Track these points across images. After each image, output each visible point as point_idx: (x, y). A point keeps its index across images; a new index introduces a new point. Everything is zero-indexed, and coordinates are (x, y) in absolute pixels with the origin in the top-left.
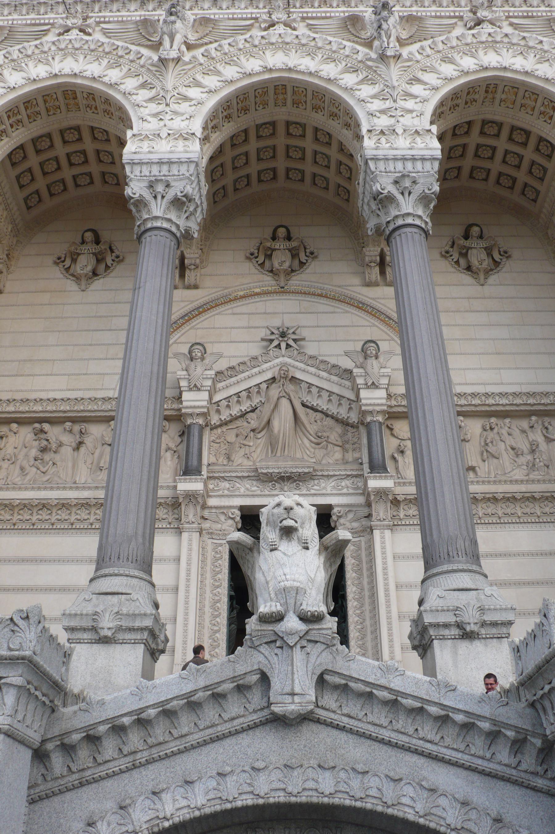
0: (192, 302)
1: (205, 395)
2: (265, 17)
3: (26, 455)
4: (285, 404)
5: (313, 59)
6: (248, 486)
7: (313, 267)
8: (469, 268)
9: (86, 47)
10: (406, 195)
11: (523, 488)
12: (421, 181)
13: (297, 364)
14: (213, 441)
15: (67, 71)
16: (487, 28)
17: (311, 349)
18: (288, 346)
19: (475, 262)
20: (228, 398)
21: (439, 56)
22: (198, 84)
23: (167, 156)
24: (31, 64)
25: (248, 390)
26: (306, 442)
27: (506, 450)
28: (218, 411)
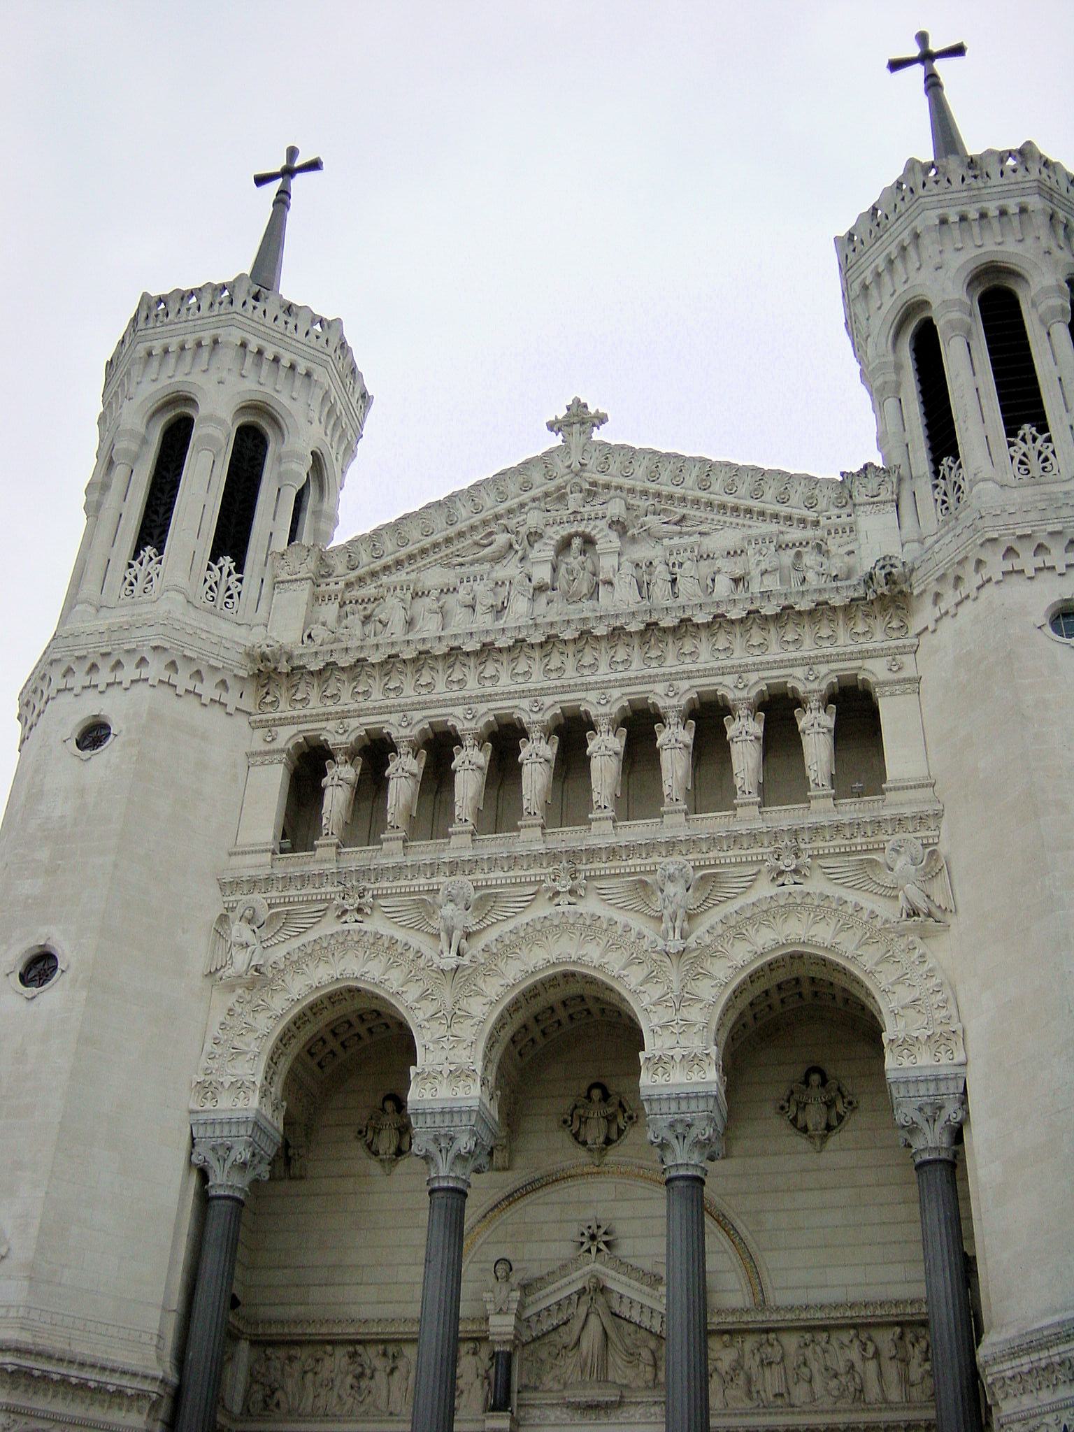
1: (510, 1320)
2: (549, 883)
3: (342, 1382)
5: (598, 944)
8: (805, 1130)
9: (365, 939)
10: (681, 1140)
12: (696, 1123)
14: (526, 1359)
15: (348, 973)
18: (599, 1250)
20: (538, 1314)
21: (732, 932)
22: (480, 993)
23: (448, 1104)
25: (558, 1304)
26: (619, 1362)
28: (529, 1327)
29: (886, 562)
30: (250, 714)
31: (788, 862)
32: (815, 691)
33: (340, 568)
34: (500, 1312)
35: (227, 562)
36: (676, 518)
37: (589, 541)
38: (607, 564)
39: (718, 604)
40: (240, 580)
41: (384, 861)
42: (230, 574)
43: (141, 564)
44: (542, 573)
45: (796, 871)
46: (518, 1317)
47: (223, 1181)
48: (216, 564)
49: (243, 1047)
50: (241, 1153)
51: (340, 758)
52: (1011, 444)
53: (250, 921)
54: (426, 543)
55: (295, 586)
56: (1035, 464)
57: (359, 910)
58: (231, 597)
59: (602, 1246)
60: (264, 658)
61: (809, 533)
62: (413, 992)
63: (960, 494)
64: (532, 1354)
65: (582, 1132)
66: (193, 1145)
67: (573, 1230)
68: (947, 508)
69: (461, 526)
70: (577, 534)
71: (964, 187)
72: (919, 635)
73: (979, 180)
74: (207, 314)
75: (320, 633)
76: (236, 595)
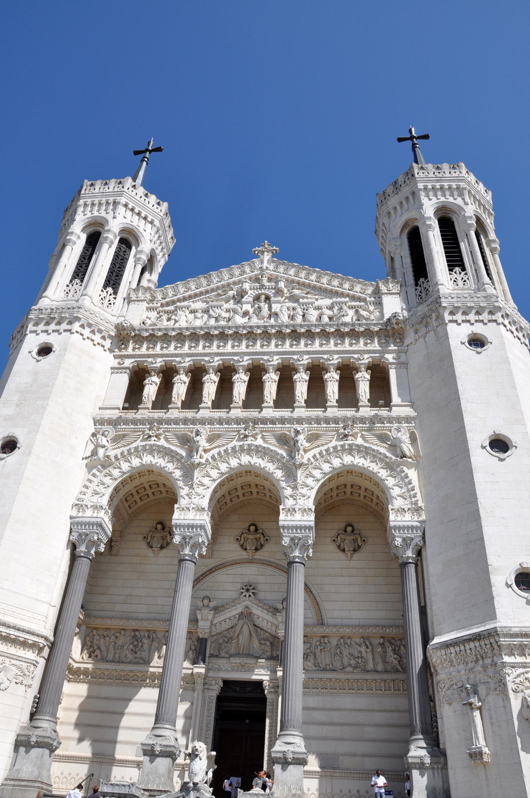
0: (207, 566)
1: (208, 624)
3: (128, 649)
4: (245, 627)
6: (226, 667)
7: (266, 548)
8: (344, 551)
11: (349, 677)
13: (253, 605)
16: (350, 441)
17: (261, 596)
18: (250, 596)
19: (346, 549)
21: (323, 459)
22: (209, 476)
24: (133, 457)
27: (346, 656)
29: (395, 315)
32: (363, 364)
33: (159, 298)
35: (110, 290)
36: (305, 292)
37: (268, 298)
38: (276, 307)
39: (323, 325)
40: (115, 298)
41: (170, 416)
42: (110, 295)
43: (73, 285)
46: (212, 623)
48: (105, 289)
49: (97, 490)
51: (153, 373)
52: (450, 274)
53: (106, 437)
54: (197, 291)
55: (139, 303)
56: (460, 283)
58: (110, 304)
59: (251, 594)
60: (124, 328)
61: (362, 303)
63: (427, 292)
64: (215, 641)
65: (245, 544)
66: (71, 532)
67: (239, 586)
68: (421, 298)
70: (263, 294)
71: (434, 176)
72: (407, 346)
73: (441, 174)
74: (112, 191)
75: (149, 322)
76: (112, 304)
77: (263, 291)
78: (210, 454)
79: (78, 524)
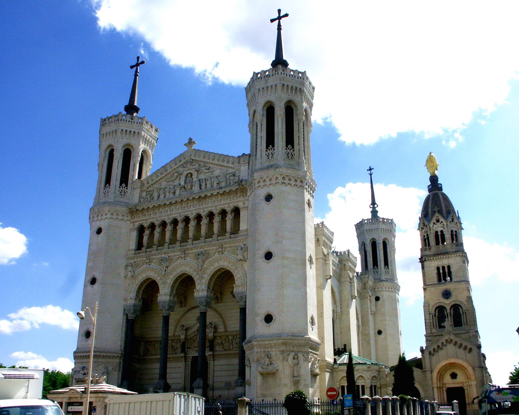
22: (169, 278)
30: (130, 220)
31: (220, 250)
34: (182, 335)
35: (124, 185)
36: (208, 168)
37: (191, 174)
40: (127, 188)
42: (124, 187)
44: (182, 183)
45: (222, 251)
47: (131, 316)
50: (132, 312)
51: (146, 229)
52: (267, 151)
54: (162, 176)
57: (149, 262)
58: (125, 193)
62: (159, 278)
69: (168, 172)
70: (190, 173)
77: (189, 171)
78: (169, 268)
79: (126, 306)
